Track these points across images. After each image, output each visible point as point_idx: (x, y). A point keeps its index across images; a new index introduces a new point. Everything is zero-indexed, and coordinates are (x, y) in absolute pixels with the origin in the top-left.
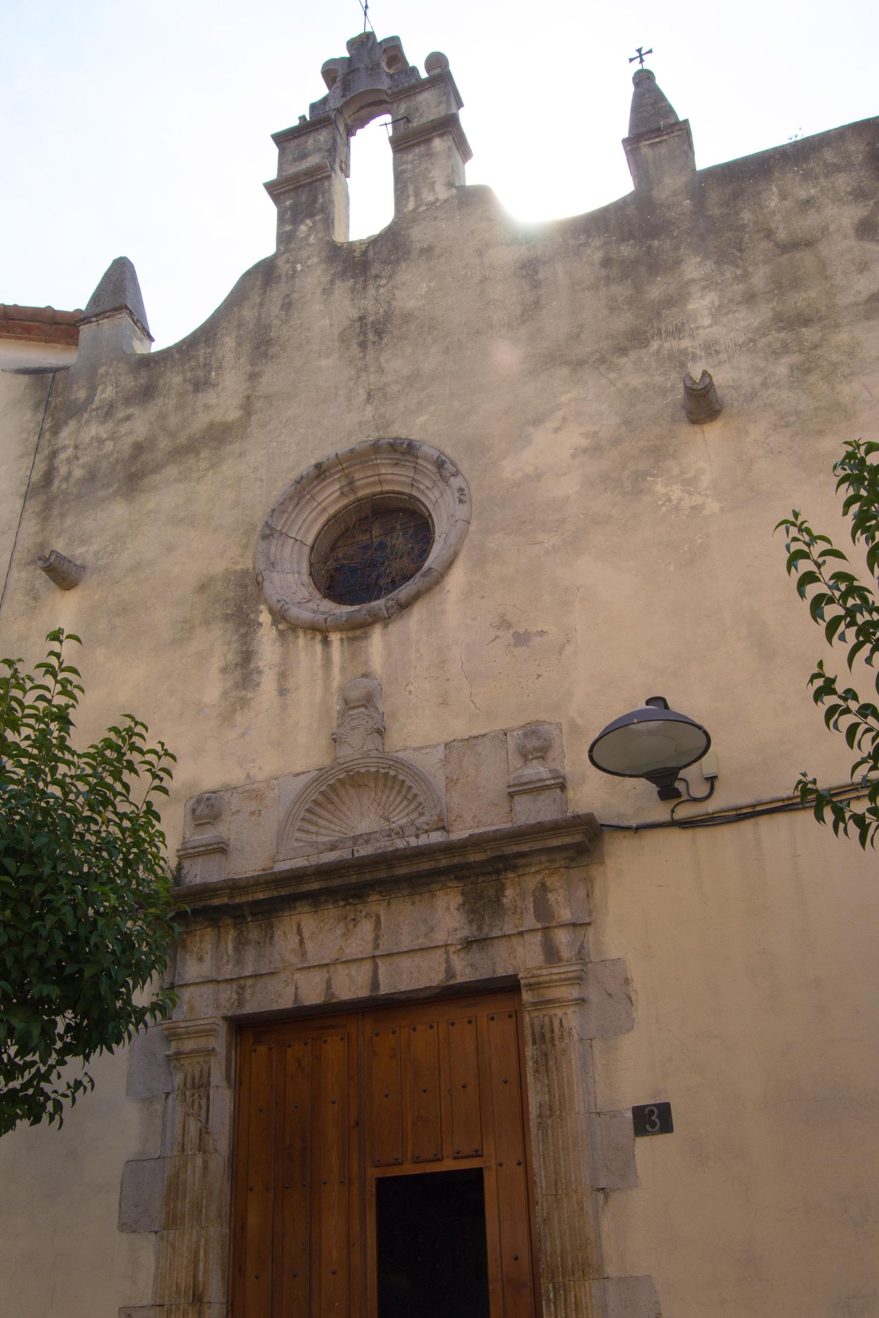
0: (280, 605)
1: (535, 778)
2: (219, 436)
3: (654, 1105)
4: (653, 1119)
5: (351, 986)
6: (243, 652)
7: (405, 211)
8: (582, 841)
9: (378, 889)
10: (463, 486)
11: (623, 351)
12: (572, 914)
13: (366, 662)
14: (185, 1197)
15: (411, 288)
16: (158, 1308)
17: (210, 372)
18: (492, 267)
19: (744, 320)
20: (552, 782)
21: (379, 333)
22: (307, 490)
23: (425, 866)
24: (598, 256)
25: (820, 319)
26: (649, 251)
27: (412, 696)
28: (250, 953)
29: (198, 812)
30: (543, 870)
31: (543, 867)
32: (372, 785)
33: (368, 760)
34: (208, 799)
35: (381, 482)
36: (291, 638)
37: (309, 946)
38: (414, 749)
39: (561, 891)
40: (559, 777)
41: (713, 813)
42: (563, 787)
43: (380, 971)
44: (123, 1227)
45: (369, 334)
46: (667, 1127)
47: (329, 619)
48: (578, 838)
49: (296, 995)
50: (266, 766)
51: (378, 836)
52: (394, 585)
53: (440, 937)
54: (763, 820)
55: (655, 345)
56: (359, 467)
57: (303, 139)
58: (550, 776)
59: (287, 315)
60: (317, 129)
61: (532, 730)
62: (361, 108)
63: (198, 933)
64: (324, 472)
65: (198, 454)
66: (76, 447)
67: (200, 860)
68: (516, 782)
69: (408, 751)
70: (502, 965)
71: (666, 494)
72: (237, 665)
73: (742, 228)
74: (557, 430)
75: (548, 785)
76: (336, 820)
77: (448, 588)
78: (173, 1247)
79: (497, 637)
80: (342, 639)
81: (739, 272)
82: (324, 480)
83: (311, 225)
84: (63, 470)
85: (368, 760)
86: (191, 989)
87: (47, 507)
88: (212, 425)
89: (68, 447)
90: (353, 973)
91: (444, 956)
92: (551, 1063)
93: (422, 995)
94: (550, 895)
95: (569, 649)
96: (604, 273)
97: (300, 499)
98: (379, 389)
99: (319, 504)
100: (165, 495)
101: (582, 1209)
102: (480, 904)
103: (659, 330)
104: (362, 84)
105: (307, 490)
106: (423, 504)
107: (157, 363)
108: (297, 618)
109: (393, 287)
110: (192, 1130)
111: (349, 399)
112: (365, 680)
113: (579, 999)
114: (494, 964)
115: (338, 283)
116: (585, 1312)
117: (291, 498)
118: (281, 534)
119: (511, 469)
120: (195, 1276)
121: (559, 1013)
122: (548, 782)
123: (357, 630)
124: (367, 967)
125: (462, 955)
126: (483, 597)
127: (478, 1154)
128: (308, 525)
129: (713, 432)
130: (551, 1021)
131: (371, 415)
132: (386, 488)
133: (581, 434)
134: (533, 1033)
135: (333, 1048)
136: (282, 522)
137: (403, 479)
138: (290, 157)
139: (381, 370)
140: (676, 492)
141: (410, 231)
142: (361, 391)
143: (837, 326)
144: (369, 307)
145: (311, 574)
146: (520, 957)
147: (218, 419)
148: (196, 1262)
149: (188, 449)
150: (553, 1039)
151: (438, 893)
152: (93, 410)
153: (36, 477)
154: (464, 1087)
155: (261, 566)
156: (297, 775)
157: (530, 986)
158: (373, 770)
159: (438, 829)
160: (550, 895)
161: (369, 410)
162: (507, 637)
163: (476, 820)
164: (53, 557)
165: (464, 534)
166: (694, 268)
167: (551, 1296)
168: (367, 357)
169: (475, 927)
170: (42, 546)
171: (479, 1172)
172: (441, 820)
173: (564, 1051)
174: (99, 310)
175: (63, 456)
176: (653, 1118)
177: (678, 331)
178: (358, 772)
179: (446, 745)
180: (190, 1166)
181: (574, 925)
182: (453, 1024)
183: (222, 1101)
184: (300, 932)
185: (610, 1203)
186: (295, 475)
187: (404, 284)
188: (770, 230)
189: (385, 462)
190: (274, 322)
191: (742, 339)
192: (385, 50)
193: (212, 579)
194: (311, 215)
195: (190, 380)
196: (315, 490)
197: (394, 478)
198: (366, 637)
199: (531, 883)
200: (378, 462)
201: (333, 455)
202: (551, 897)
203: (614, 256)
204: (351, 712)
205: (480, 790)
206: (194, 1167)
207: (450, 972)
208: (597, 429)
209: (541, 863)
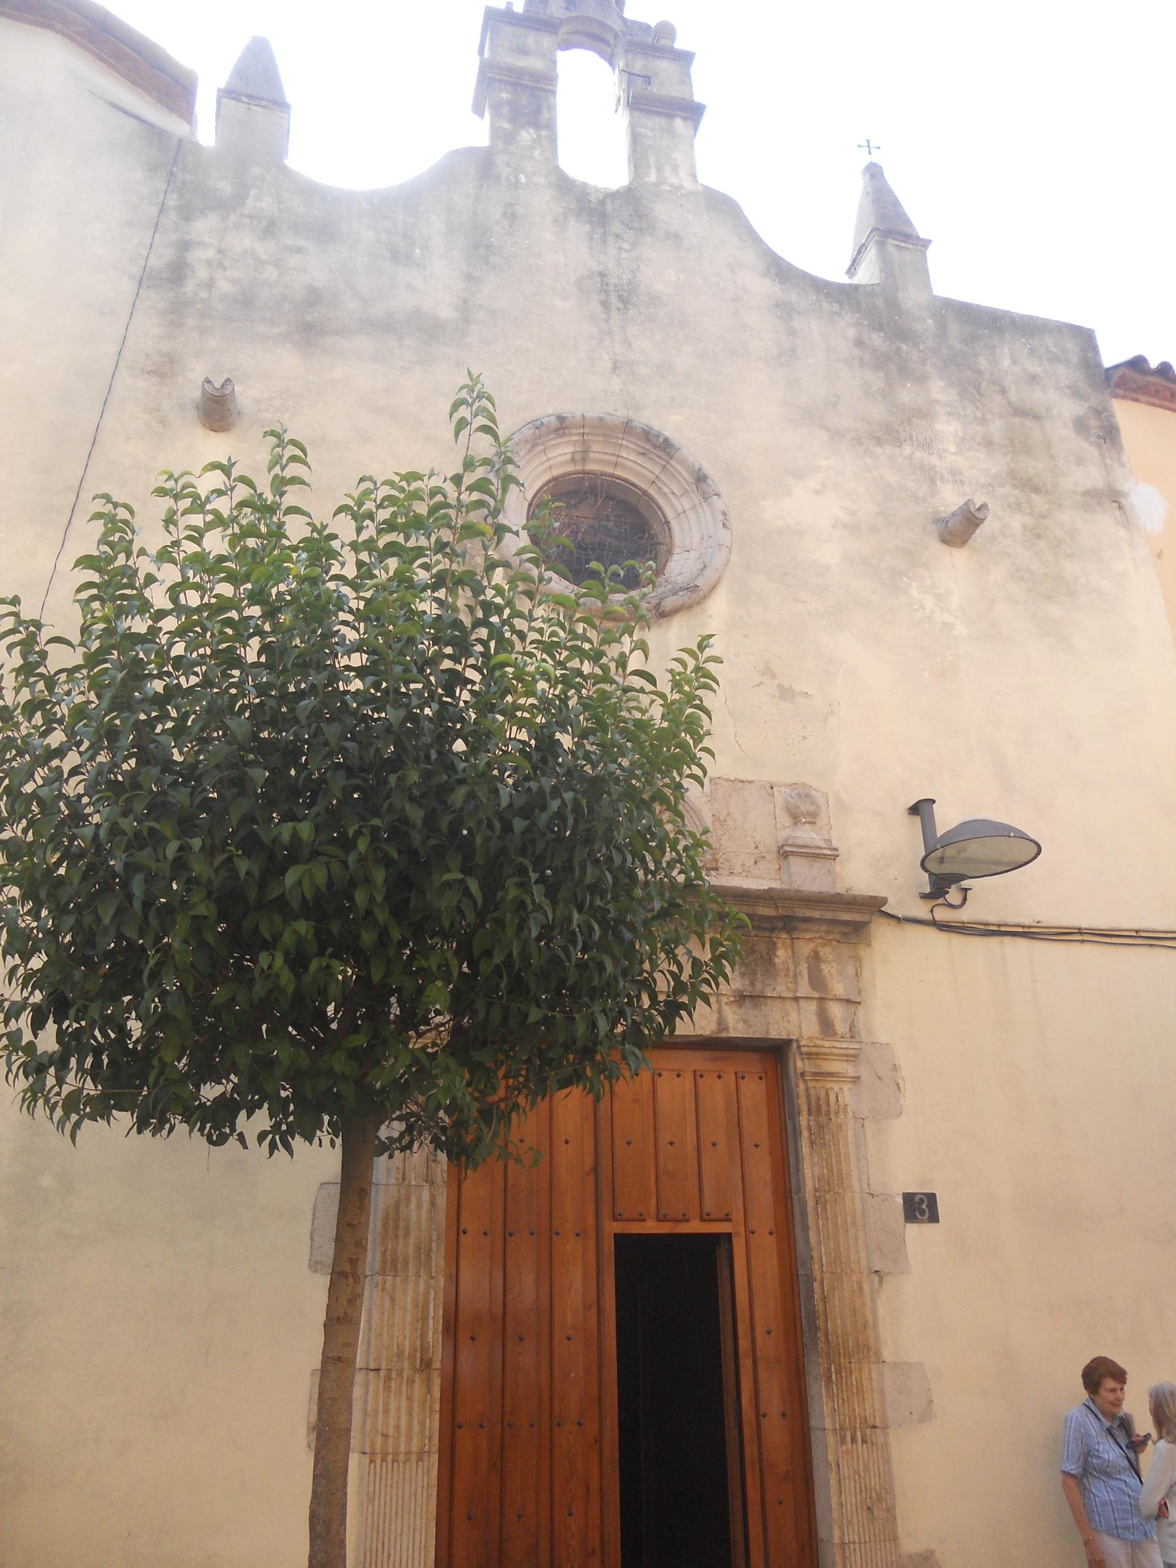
4: (921, 1207)
7: (647, 179)
8: (852, 919)
11: (879, 442)
14: (407, 1235)
16: (372, 1374)
21: (625, 302)
24: (851, 332)
25: (1047, 492)
39: (834, 964)
42: (834, 857)
46: (934, 1218)
54: (1007, 940)
55: (907, 449)
60: (539, 30)
61: (805, 794)
62: (577, 32)
66: (220, 251)
68: (790, 842)
73: (980, 373)
82: (561, 436)
84: (202, 273)
96: (857, 352)
97: (534, 446)
101: (861, 1289)
102: (751, 958)
103: (911, 438)
106: (660, 509)
114: (768, 1024)
115: (572, 221)
117: (526, 442)
120: (423, 1336)
121: (836, 1087)
122: (826, 852)
125: (735, 1008)
127: (727, 1219)
129: (959, 558)
130: (827, 1094)
132: (619, 473)
134: (809, 1105)
137: (645, 472)
140: (929, 603)
143: (1060, 505)
148: (425, 1319)
149: (386, 327)
154: (714, 1145)
157: (810, 1055)
160: (823, 966)
161: (616, 384)
166: (939, 390)
169: (747, 982)
171: (728, 1237)
176: (924, 1206)
177: (927, 445)
180: (414, 1200)
181: (848, 1001)
182: (701, 1076)
186: (530, 416)
191: (982, 480)
194: (537, 126)
197: (634, 468)
201: (578, 415)
202: (825, 968)
203: (866, 341)
206: (419, 1200)
207: (722, 1023)
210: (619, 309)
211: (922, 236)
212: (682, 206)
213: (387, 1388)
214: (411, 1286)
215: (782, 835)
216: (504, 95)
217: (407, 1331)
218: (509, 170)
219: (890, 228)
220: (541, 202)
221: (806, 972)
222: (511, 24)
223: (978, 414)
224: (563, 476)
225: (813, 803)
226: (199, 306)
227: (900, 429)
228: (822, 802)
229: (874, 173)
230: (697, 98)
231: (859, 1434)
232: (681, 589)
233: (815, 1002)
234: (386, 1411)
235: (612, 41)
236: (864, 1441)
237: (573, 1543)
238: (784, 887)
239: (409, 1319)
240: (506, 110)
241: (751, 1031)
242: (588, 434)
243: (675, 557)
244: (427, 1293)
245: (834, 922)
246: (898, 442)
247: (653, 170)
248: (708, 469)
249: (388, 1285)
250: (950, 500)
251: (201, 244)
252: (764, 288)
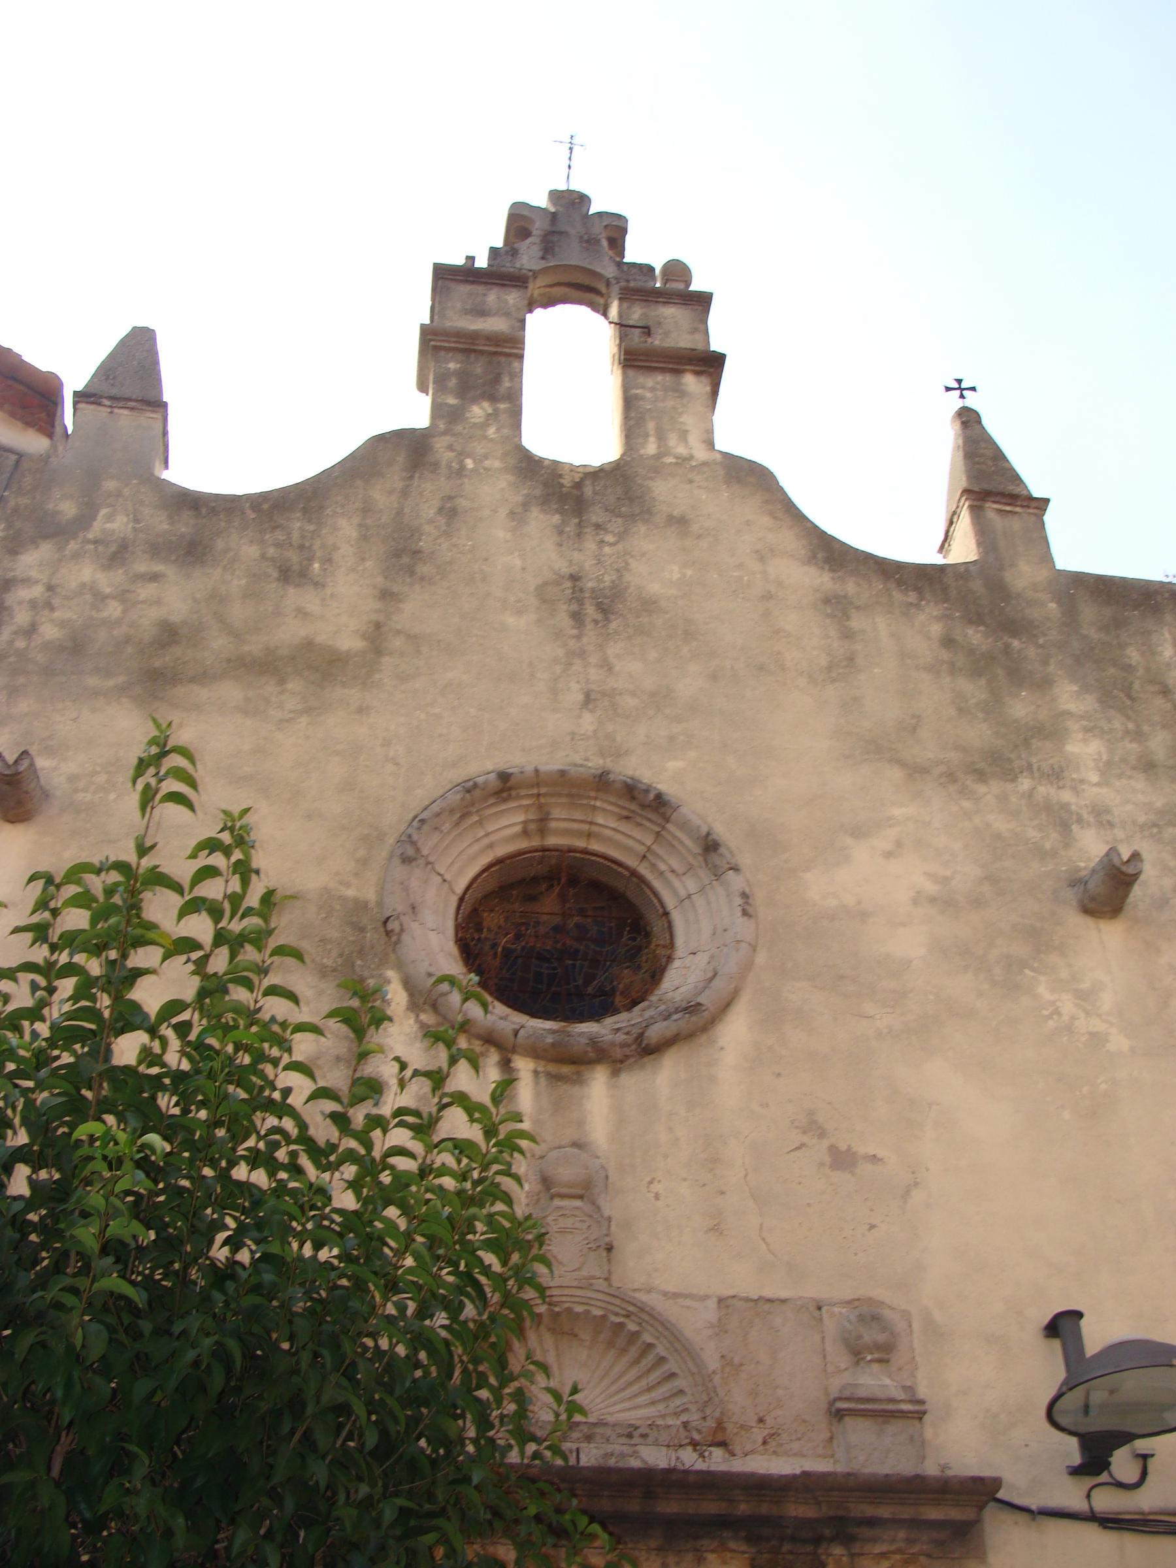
1: (880, 1394)
2: (321, 667)
7: (642, 452)
10: (747, 890)
11: (982, 776)
13: (581, 1123)
15: (654, 566)
17: (311, 560)
18: (780, 584)
19: (1143, 793)
21: (606, 611)
23: (711, 1507)
24: (936, 629)
26: (1007, 648)
27: (660, 1204)
30: (893, 1553)
31: (893, 1548)
33: (590, 1294)
35: (589, 835)
38: (665, 1294)
42: (920, 1416)
45: (587, 606)
47: (522, 1033)
48: (968, 1514)
51: (608, 1431)
55: (1025, 784)
56: (564, 800)
57: (480, 289)
59: (448, 524)
60: (503, 285)
61: (869, 1314)
64: (510, 789)
65: (282, 681)
66: (50, 588)
68: (847, 1393)
69: (654, 1295)
71: (1053, 1003)
72: (338, 1058)
73: (1129, 669)
74: (888, 855)
75: (902, 1412)
77: (721, 1043)
79: (801, 1146)
80: (536, 1073)
81: (1131, 726)
82: (505, 800)
83: (490, 411)
84: (22, 617)
85: (590, 1294)
88: (309, 645)
89: (37, 582)
95: (918, 1196)
96: (945, 655)
97: (464, 816)
98: (604, 694)
99: (487, 835)
103: (1030, 767)
104: (573, 255)
107: (213, 511)
109: (626, 553)
111: (554, 691)
112: (575, 1150)
115: (535, 513)
117: (452, 811)
118: (428, 863)
119: (823, 887)
126: (779, 1074)
129: (1109, 937)
131: (592, 728)
132: (595, 846)
133: (925, 873)
137: (630, 842)
138: (459, 305)
139: (607, 666)
140: (1067, 1005)
141: (651, 483)
142: (574, 686)
144: (587, 565)
147: (320, 639)
149: (267, 666)
152: (89, 542)
155: (395, 903)
158: (599, 1313)
161: (588, 722)
165: (748, 966)
166: (1069, 697)
168: (585, 640)
174: (114, 391)
175: (24, 594)
177: (1056, 775)
178: (569, 1310)
179: (720, 1300)
187: (644, 554)
188: (1166, 686)
190: (427, 528)
191: (1142, 819)
192: (606, 227)
194: (493, 398)
195: (273, 560)
197: (615, 838)
198: (578, 1080)
200: (598, 804)
201: (529, 768)
203: (959, 638)
204: (557, 1202)
205: (780, 1392)
208: (948, 873)
209: (893, 1541)
210: (596, 622)
211: (1035, 495)
212: (691, 482)
215: (836, 1384)
216: (452, 366)
218: (452, 454)
219: (991, 486)
220: (494, 491)
222: (467, 282)
223: (1131, 726)
225: (884, 1329)
226: (12, 659)
227: (1012, 756)
228: (901, 1326)
229: (968, 419)
230: (715, 346)
232: (677, 1011)
235: (603, 290)
238: (840, 1468)
240: (453, 382)
242: (545, 795)
243: (676, 963)
245: (916, 1524)
246: (1011, 776)
247: (652, 439)
248: (721, 831)
250: (1091, 847)
251: (27, 581)
252: (806, 578)
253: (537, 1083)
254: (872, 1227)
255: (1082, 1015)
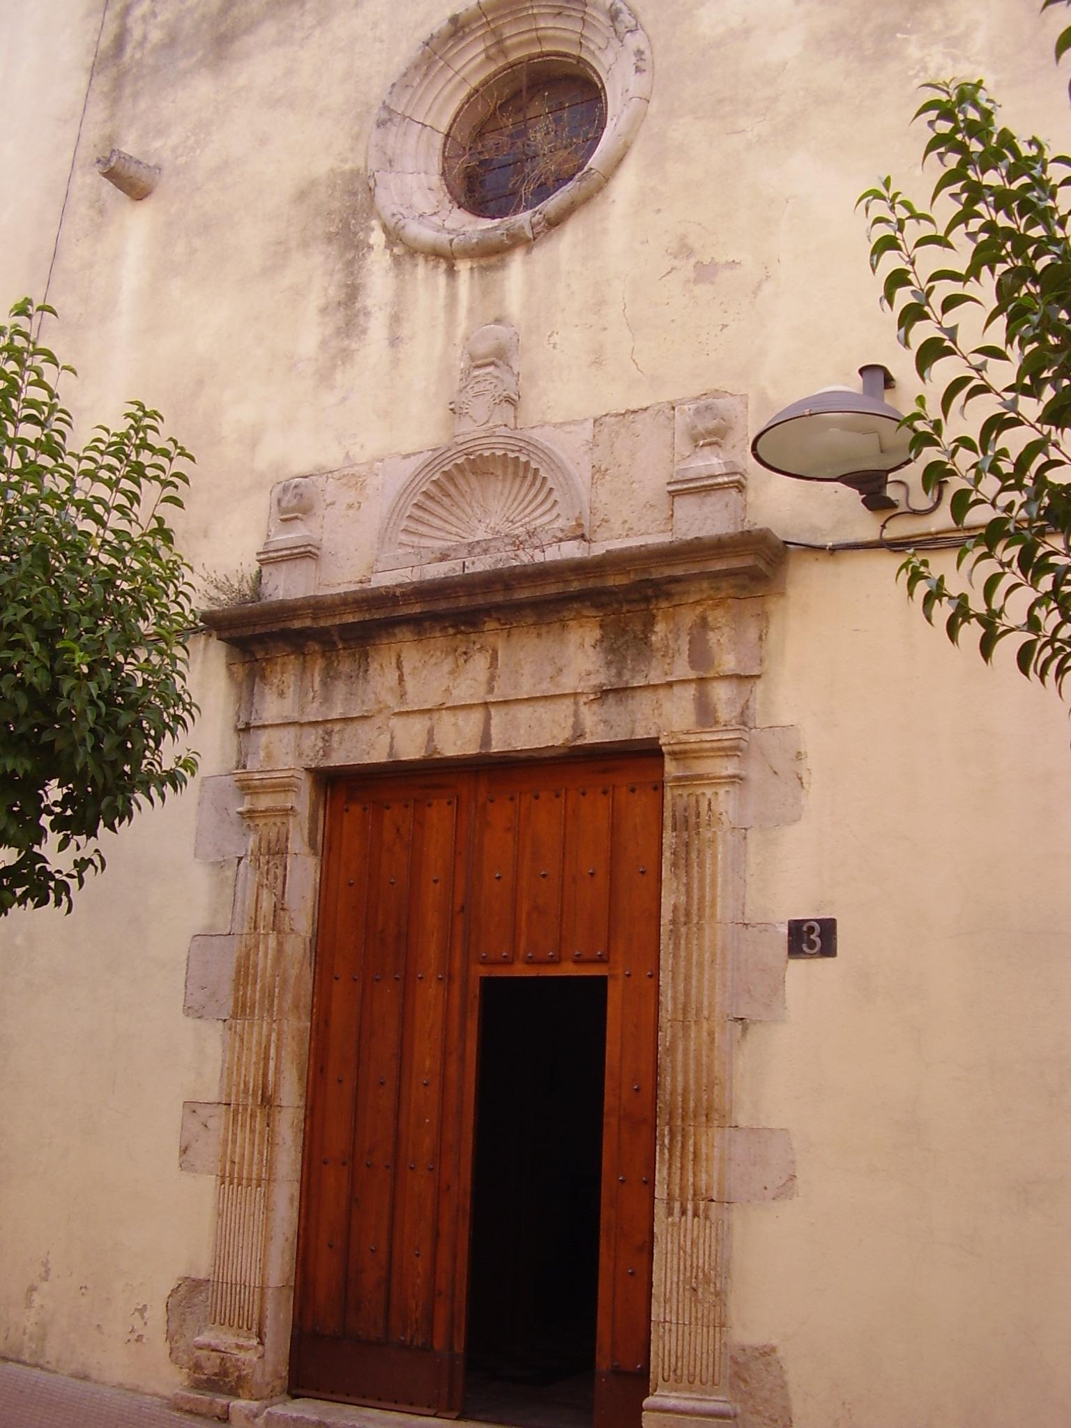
0: (395, 220)
1: (705, 474)
3: (816, 920)
4: (812, 938)
5: (457, 739)
6: (348, 286)
9: (495, 615)
12: (739, 662)
20: (726, 479)
22: (440, 53)
23: (552, 589)
28: (340, 688)
29: (284, 504)
31: (705, 596)
32: (499, 473)
34: (296, 487)
36: (408, 266)
37: (410, 684)
38: (555, 426)
39: (726, 630)
40: (736, 473)
41: (937, 533)
43: (493, 722)
44: (190, 1010)
46: (828, 950)
49: (392, 747)
50: (371, 442)
52: (543, 192)
53: (569, 683)
56: (510, 19)
58: (725, 471)
63: (279, 660)
64: (462, 27)
67: (284, 566)
69: (547, 428)
70: (643, 724)
72: (339, 303)
75: (719, 484)
76: (452, 519)
78: (242, 1040)
80: (472, 269)
82: (462, 38)
84: (137, 34)
86: (269, 731)
87: (118, 84)
90: (461, 723)
91: (573, 708)
92: (694, 855)
93: (546, 754)
94: (711, 634)
95: (767, 289)
99: (457, 73)
100: (260, 66)
105: (440, 53)
106: (595, 72)
108: (415, 239)
110: (264, 904)
113: (734, 777)
114: (634, 722)
116: (704, 1164)
117: (417, 67)
120: (265, 1075)
121: (709, 792)
122: (720, 480)
123: (491, 254)
124: (477, 716)
125: (595, 707)
126: (659, 210)
127: (601, 960)
128: (442, 104)
130: (697, 801)
132: (547, 48)
134: (674, 816)
135: (439, 816)
136: (405, 101)
137: (567, 35)
145: (443, 174)
146: (665, 717)
148: (266, 1059)
150: (698, 825)
151: (571, 623)
153: (106, 42)
154: (592, 874)
155: (373, 166)
156: (407, 456)
157: (677, 756)
159: (575, 538)
162: (686, 269)
163: (627, 526)
164: (114, 159)
167: (667, 1141)
169: (613, 671)
170: (111, 139)
171: (602, 982)
172: (580, 525)
173: (712, 842)
176: (812, 937)
179: (595, 421)
183: (304, 873)
184: (399, 667)
185: (748, 1037)
186: (423, 34)
189: (543, 11)
193: (313, 183)
196: (450, 55)
198: (502, 265)
199: (688, 617)
204: (476, 373)
206: (267, 948)
213: (235, 1120)
214: (256, 1029)
217: (252, 1069)
221: (685, 647)
224: (484, 83)
231: (690, 1206)
233: (694, 685)
234: (234, 1142)
236: (696, 1215)
237: (419, 1281)
239: (254, 1059)
241: (612, 732)
244: (269, 1036)
249: (239, 1028)
253: (472, 278)
254: (724, 326)
255: (950, 62)
